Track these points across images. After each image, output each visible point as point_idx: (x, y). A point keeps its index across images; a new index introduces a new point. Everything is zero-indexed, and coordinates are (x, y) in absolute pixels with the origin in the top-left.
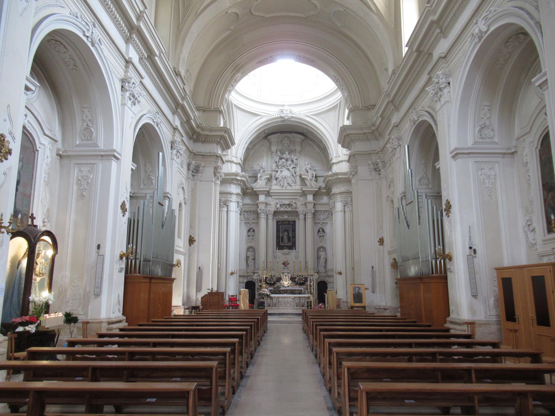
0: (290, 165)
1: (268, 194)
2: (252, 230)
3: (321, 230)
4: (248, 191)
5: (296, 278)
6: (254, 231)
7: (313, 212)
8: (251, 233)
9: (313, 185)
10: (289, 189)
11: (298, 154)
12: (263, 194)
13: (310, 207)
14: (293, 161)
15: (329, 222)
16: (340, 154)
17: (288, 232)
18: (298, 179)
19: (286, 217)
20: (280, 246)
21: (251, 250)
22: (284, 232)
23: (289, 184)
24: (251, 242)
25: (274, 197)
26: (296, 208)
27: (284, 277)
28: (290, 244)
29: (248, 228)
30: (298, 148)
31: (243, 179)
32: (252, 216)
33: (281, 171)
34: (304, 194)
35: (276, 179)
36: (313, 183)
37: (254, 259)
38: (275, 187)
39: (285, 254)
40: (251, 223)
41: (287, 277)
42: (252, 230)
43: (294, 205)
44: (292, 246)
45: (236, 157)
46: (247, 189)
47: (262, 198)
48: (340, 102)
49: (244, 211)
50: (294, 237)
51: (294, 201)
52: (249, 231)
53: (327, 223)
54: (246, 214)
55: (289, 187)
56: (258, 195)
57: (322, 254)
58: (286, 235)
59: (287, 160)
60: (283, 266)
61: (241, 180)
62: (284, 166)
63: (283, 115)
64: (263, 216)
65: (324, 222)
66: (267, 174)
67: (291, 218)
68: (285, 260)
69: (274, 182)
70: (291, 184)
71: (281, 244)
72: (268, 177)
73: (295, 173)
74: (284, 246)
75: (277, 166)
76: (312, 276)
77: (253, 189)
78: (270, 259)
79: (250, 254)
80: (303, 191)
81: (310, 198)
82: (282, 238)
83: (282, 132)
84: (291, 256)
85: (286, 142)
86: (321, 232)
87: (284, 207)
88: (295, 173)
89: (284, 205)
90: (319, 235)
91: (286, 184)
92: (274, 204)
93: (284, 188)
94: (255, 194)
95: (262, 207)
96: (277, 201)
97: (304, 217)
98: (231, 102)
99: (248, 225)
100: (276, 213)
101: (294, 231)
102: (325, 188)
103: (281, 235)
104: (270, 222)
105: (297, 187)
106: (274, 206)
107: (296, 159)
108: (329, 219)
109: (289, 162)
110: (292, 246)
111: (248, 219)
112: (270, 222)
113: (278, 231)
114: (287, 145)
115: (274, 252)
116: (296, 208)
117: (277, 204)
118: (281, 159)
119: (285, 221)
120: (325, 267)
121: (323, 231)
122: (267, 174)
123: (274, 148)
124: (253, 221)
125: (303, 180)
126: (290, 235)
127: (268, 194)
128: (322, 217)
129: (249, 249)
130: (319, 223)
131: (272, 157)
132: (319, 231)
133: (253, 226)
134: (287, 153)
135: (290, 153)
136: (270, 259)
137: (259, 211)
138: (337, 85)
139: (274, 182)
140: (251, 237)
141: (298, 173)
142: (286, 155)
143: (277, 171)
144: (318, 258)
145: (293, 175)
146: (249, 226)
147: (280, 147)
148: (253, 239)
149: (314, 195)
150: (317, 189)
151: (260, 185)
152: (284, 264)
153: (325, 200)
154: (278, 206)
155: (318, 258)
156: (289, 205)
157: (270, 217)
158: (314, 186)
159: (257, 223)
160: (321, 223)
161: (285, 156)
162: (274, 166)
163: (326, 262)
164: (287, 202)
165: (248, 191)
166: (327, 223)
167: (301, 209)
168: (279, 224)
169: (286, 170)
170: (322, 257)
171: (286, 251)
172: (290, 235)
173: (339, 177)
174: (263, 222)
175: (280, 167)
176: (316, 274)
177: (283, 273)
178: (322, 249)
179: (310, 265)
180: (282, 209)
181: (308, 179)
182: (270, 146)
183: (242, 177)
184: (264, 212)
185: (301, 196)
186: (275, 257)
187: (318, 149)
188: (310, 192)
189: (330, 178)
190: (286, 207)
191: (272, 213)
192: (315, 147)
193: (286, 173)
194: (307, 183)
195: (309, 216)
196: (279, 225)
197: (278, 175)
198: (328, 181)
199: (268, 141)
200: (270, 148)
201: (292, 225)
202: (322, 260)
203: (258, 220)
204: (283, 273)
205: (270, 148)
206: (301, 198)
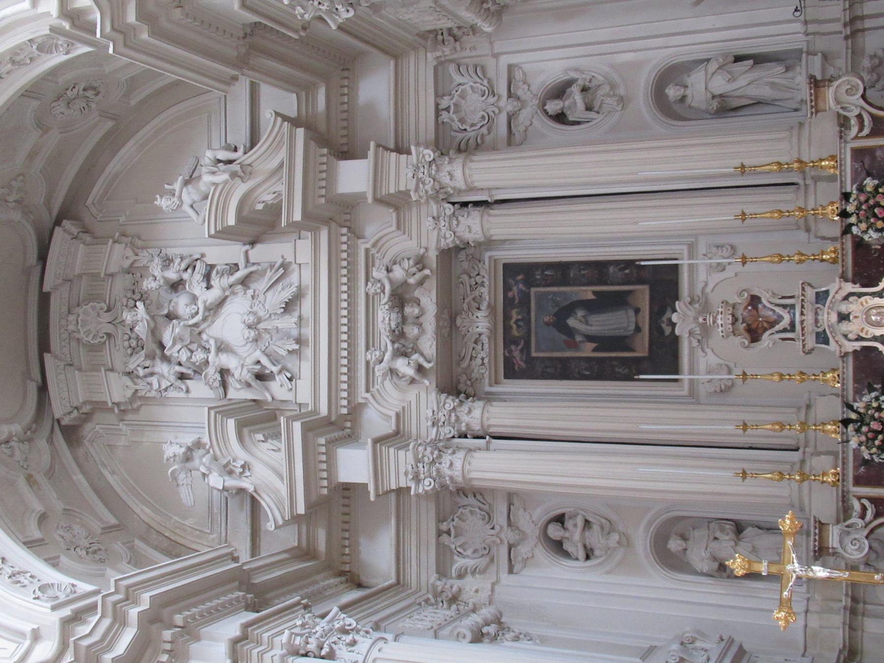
0: (194, 299)
1: (337, 427)
2: (555, 532)
3: (553, 107)
4: (322, 547)
5: (859, 245)
6: (560, 519)
7: (429, 154)
8: (574, 536)
9: (274, 163)
10: (317, 309)
11: (143, 258)
12: (331, 462)
13: (402, 173)
14: (176, 286)
15: (505, 60)
17: (569, 309)
18: (263, 253)
19: (480, 323)
20: (664, 356)
21: (674, 545)
22: (570, 332)
23: (288, 307)
24: (626, 542)
25: (362, 395)
26: (421, 262)
27: (851, 328)
28: (643, 295)
29: (542, 554)
30: (117, 256)
31: (133, 613)
32: (474, 528)
33: (222, 348)
34: (337, 216)
35: (261, 377)
36: (266, 159)
37: (739, 528)
38: (305, 388)
39: (706, 330)
40: (509, 536)
41: (854, 307)
42: (555, 532)
43: (398, 273)
44: (663, 282)
45: (36, 636)
46: (305, 553)
47: (354, 465)
49: (442, 572)
50: (597, 270)
51: (378, 273)
52: (558, 547)
53: (510, 68)
54: (460, 562)
55: (306, 306)
56: (349, 491)
57: (700, 87)
58: (594, 323)
59: (171, 317)
60: (767, 339)
61: (153, 620)
62: (196, 332)
64: (457, 466)
65: (504, 92)
66: (218, 431)
67: (490, 290)
68: (723, 320)
69: (278, 389)
70: (287, 294)
71: (642, 348)
72: (231, 423)
73: (235, 267)
74: (656, 329)
75: (199, 370)
76: (843, 123)
77: (296, 519)
78: (721, 424)
79: (699, 556)
80: (312, 220)
81: (353, 177)
82: (604, 342)
83: (44, 346)
84: (712, 283)
85: (91, 322)
86: (565, 106)
87: (412, 331)
88: (235, 267)
89: (398, 335)
90: (577, 111)
91: (288, 323)
92: (401, 398)
93: (308, 332)
94: (336, 505)
95: (400, 466)
96: (379, 370)
97: (475, 213)
99: (523, 550)
100: (455, 385)
101: (562, 272)
102: (304, 90)
103: (587, 350)
104: (500, 416)
105: (303, 256)
106: (411, 395)
107: (167, 262)
108: (490, 63)
109: (181, 304)
110: (663, 282)
111: (488, 552)
112: (500, 416)
113: (563, 370)
114: (106, 317)
115: (693, 397)
116: (421, 262)
117: (393, 372)
118: (162, 347)
119: (507, 329)
120: (784, 59)
121: (560, 91)
122: (218, 431)
123: (117, 389)
124: (501, 519)
125: (258, 226)
126: (587, 293)
127: (337, 427)
128: (475, 105)
129: (672, 562)
130: (511, 118)
131: (161, 399)
132: (560, 118)
133: (530, 521)
134: (128, 317)
135: (137, 295)
136: (721, 424)
137: (427, 485)
138: (342, 194)
139: (278, 389)
140: (595, 538)
141: (233, 252)
142: (139, 317)
143: (224, 372)
144: (725, 108)
145: (244, 282)
146: (532, 547)
147: (116, 355)
148: (609, 528)
149: (347, 154)
150: (300, 132)
151: (272, 471)
152: (754, 334)
153: (375, 89)
154: (404, 367)
155: (725, 108)
156: (400, 298)
157: (474, 415)
158: (283, 154)
159: (511, 497)
160: (508, 106)
161: (141, 329)
162: (199, 389)
163: (759, 59)
164: (385, 318)
165: (322, 547)
166: (510, 68)
167: (428, 233)
168: (524, 362)
169: (219, 322)
170: (720, 85)
171: (683, 320)
172: (587, 293)
174: (492, 466)
175: (199, 356)
176: (830, 93)
177: (822, 338)
178: (672, 92)
179: (760, 147)
180: (429, 345)
181: (241, 189)
182: (99, 407)
183: (120, 620)
184: (429, 454)
185: (356, 234)
186: (726, 390)
187: (128, 150)
188: (317, 180)
189: (131, 17)
190: (417, 321)
191: (450, 403)
192: (114, 166)
193: (230, 326)
194: (269, 198)
195: (457, 174)
196: (530, 360)
197: (239, 365)
198: (157, 32)
199: (87, 417)
200: (124, 410)
201: (530, 283)
202: (746, 83)
203: (493, 491)
204: (822, 338)
205: (124, 410)
206: (371, 231)
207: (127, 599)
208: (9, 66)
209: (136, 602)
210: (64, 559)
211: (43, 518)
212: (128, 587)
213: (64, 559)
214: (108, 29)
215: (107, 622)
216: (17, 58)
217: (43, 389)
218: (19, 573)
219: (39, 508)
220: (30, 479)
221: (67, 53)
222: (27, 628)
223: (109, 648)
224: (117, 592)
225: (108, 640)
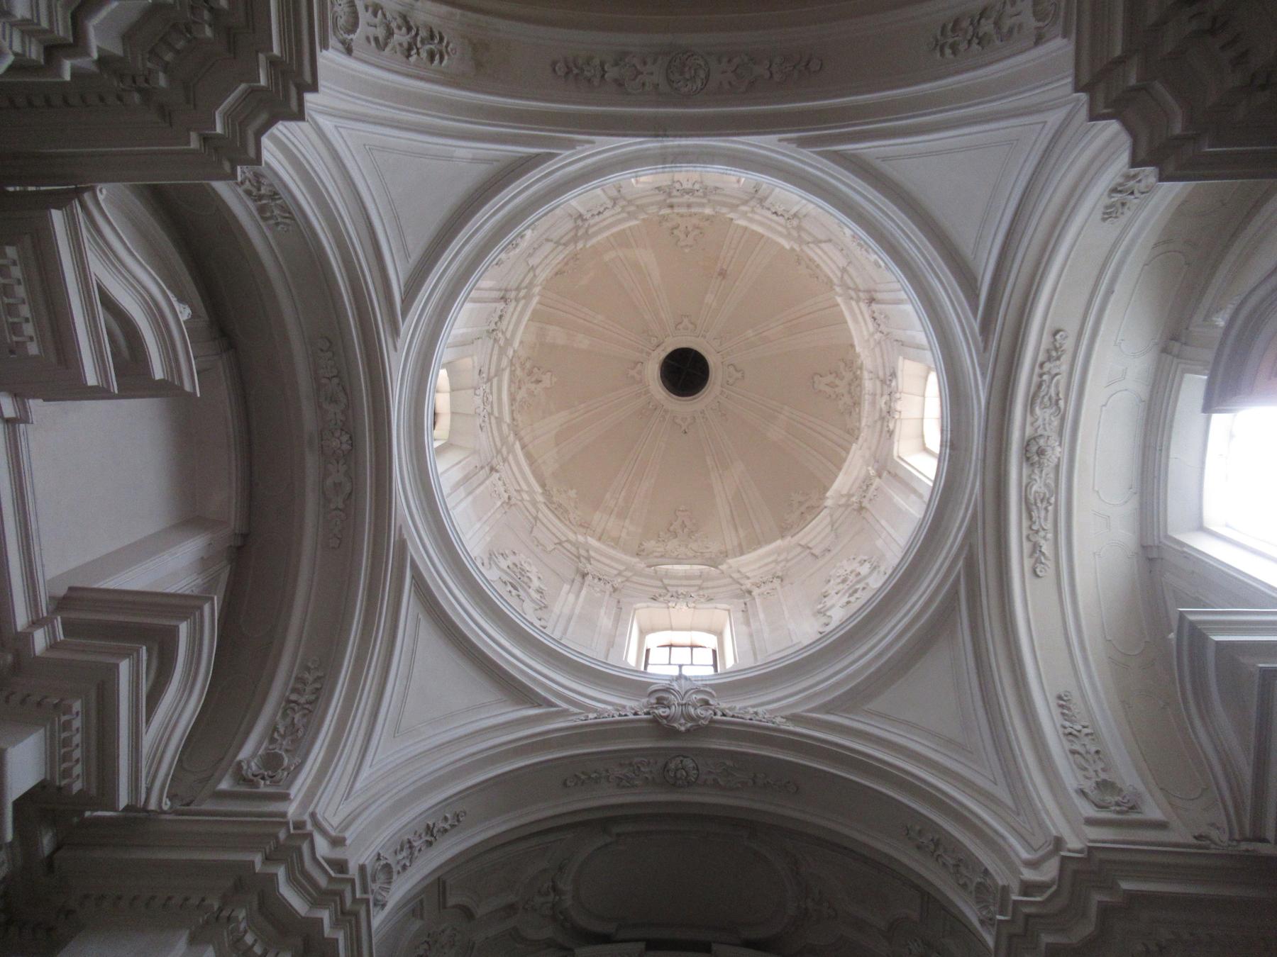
16: (1058, 825)
45: (337, 842)
48: (971, 564)
63: (661, 711)
98: (402, 546)
173: (1125, 885)
207: (343, 913)
208: (951, 861)
209: (336, 924)
210: (417, 925)
211: (467, 913)
212: (356, 915)
213: (417, 925)
214: (1027, 910)
215: (323, 882)
216: (963, 870)
217: (606, 939)
218: (412, 854)
219: (480, 912)
220: (511, 909)
221: (982, 922)
222: (350, 835)
223: (292, 879)
224: (354, 900)
225: (300, 879)
